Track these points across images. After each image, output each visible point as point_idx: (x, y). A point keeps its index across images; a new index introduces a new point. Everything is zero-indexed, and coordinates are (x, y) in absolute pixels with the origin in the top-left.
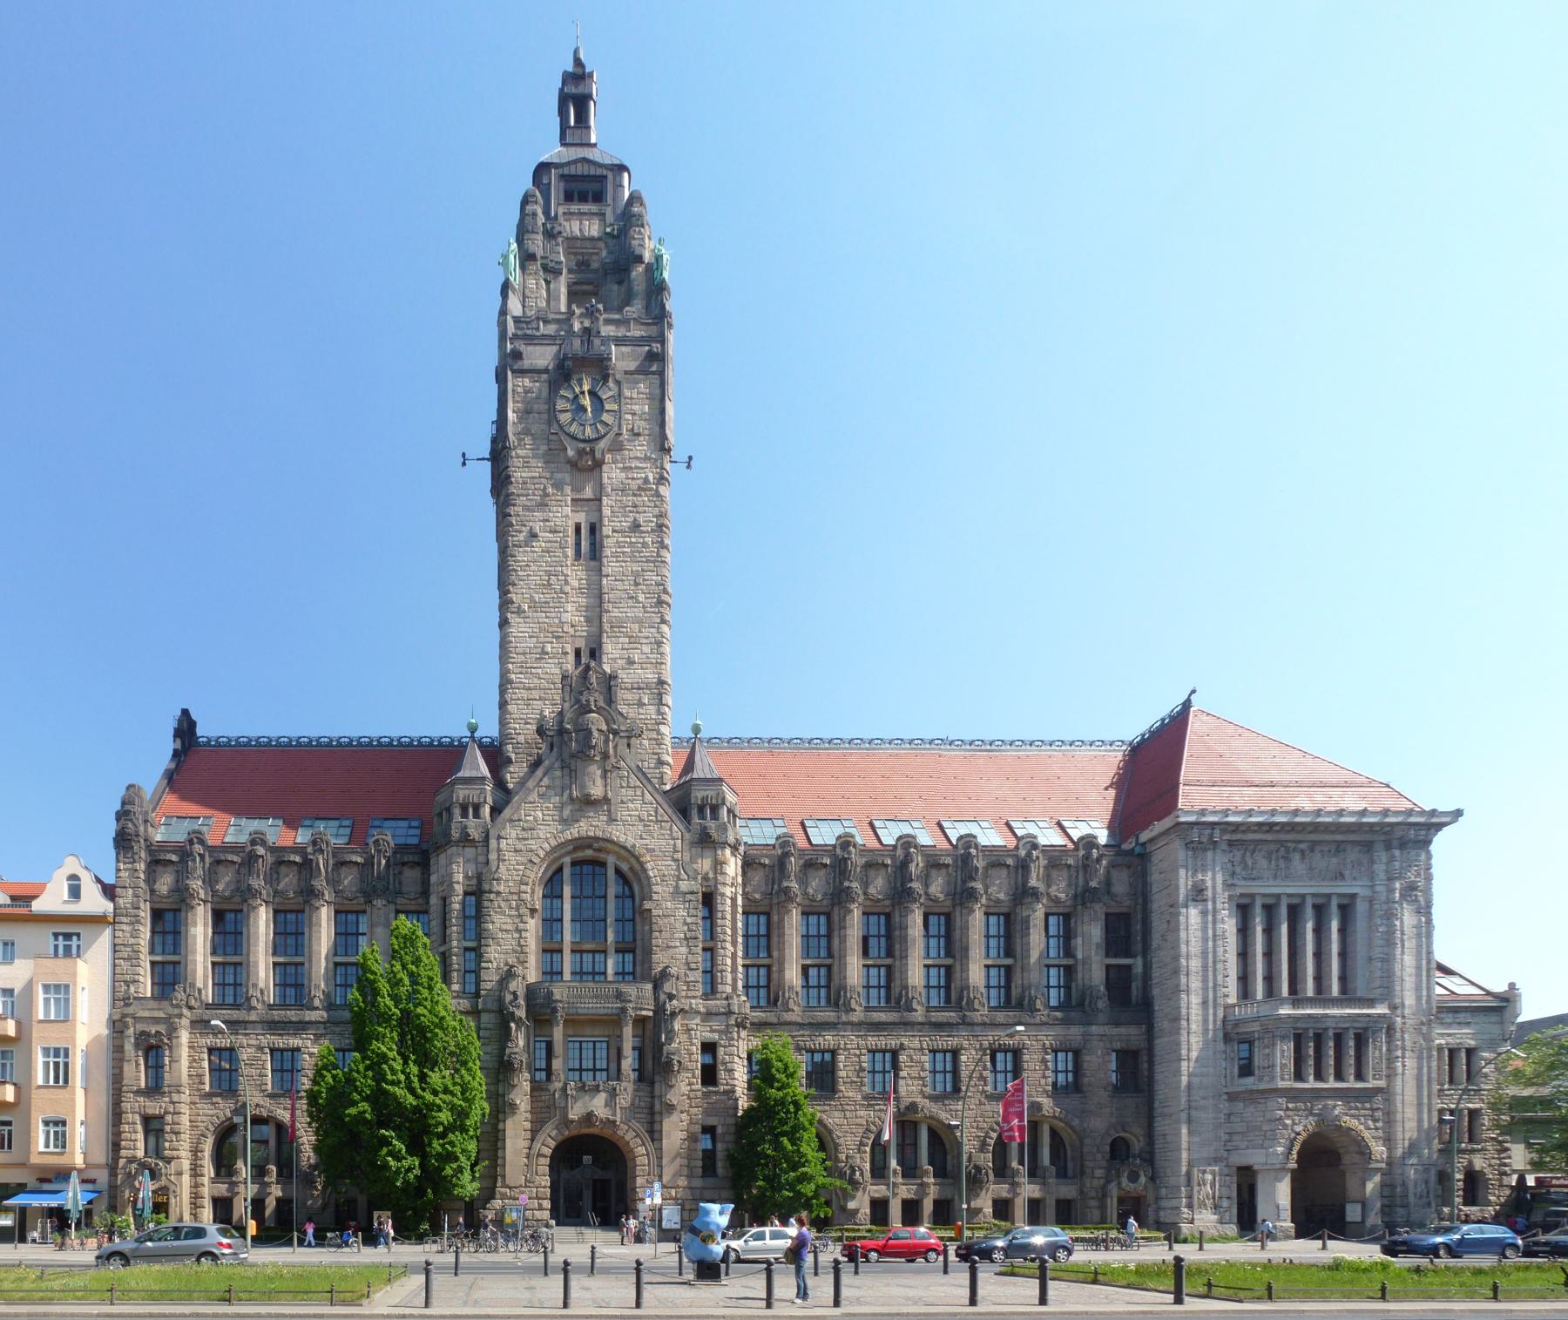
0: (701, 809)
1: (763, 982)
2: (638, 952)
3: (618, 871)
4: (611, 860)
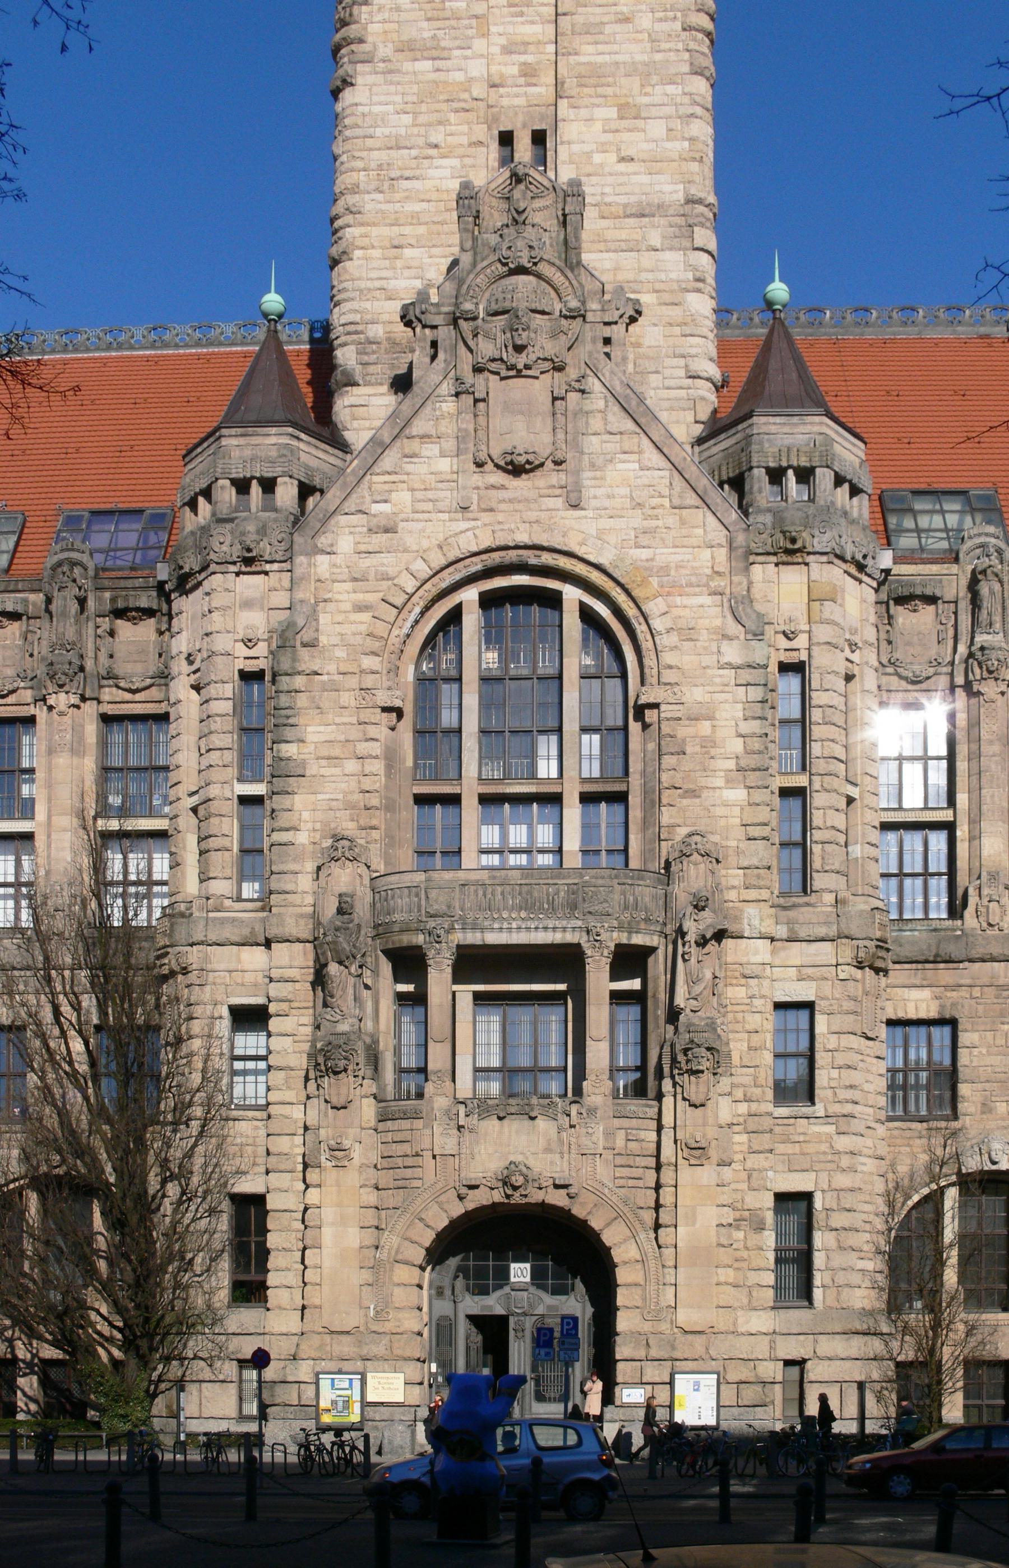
0: (776, 476)
1: (938, 863)
2: (635, 800)
3: (587, 615)
4: (571, 595)
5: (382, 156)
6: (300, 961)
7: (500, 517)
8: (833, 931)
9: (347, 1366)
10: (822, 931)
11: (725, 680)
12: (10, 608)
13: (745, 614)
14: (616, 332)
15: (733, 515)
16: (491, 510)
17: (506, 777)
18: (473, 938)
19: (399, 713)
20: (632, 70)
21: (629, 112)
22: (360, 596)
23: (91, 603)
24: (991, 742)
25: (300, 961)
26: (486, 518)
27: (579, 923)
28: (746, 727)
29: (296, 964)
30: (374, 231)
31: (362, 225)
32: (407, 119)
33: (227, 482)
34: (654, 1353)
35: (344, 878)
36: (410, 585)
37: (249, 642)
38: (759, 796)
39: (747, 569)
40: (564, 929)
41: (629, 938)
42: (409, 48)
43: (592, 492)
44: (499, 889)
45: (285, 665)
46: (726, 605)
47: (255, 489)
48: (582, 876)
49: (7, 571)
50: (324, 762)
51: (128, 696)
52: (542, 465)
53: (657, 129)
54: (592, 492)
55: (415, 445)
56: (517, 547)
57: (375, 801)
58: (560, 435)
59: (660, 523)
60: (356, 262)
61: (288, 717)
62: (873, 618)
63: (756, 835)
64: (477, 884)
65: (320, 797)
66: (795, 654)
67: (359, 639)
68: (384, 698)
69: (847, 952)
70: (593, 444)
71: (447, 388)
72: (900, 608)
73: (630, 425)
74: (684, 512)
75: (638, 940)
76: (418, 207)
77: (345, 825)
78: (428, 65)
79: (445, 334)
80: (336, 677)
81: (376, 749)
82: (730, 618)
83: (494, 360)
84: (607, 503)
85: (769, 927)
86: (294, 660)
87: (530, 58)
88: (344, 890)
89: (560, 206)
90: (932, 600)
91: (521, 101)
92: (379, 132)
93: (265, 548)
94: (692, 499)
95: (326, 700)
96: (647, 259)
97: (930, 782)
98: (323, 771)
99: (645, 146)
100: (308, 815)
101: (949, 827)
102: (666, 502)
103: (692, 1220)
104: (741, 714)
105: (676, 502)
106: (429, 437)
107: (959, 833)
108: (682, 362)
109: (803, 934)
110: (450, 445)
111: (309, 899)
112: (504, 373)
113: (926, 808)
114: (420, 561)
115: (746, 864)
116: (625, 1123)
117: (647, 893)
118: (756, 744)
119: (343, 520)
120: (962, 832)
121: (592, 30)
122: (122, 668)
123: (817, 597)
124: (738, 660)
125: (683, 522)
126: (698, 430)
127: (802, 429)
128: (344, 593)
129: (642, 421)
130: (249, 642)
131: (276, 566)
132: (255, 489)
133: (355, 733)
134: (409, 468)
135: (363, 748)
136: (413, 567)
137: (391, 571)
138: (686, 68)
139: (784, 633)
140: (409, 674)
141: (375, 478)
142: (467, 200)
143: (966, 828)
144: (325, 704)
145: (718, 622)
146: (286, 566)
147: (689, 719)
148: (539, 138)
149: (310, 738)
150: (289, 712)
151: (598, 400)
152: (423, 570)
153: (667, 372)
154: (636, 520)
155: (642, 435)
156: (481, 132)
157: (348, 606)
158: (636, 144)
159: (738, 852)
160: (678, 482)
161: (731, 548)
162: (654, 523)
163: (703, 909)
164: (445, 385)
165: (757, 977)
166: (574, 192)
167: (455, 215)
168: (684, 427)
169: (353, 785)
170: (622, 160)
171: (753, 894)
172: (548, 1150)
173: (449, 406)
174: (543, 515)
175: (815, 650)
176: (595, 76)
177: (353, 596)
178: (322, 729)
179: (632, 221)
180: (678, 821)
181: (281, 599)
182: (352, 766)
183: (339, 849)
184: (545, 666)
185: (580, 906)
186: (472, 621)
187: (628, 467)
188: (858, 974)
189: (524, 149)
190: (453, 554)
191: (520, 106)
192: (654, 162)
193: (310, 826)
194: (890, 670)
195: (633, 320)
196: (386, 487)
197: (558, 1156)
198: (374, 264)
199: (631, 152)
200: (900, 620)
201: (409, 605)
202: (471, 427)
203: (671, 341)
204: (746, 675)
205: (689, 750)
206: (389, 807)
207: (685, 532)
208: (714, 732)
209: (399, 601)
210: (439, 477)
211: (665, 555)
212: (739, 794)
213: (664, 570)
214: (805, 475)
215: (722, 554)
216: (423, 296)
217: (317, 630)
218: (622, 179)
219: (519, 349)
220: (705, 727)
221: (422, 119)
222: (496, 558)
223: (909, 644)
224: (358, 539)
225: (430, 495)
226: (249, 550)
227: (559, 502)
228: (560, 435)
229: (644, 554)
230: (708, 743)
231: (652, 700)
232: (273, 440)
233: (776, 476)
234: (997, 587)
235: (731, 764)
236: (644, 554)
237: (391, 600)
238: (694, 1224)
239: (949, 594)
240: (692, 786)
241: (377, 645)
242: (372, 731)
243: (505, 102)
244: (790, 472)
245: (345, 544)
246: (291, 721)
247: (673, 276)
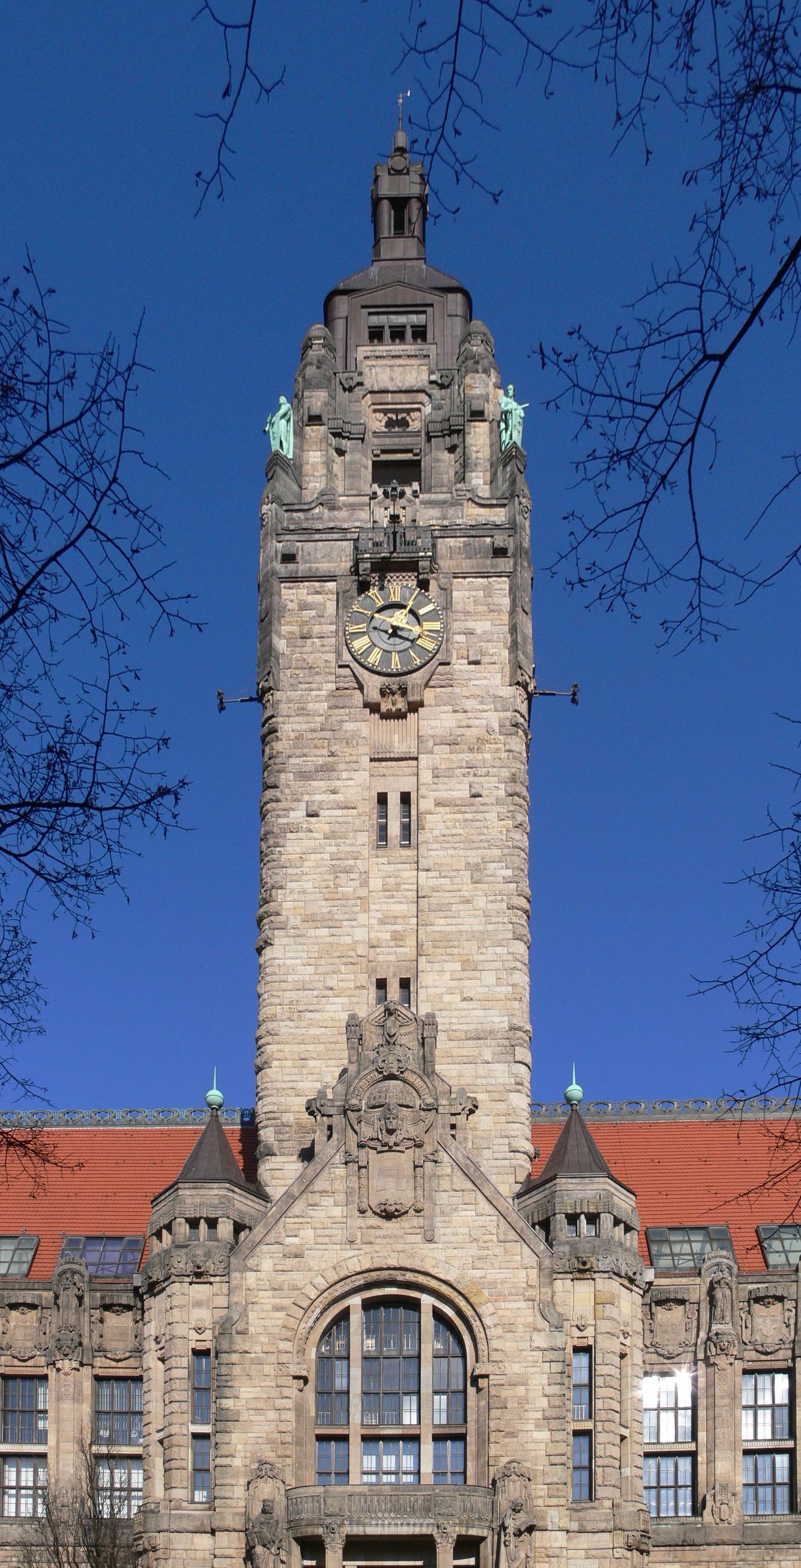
0: (572, 1219)
1: (685, 1478)
2: (471, 1439)
3: (438, 1315)
4: (427, 1301)
5: (293, 995)
6: (236, 1544)
7: (377, 1248)
8: (611, 1525)
10: (603, 1526)
11: (535, 1359)
12: (29, 1301)
13: (551, 1315)
14: (460, 1120)
15: (542, 1247)
16: (371, 1243)
17: (381, 1423)
18: (358, 1530)
19: (306, 1380)
20: (472, 936)
21: (469, 966)
22: (278, 1301)
23: (86, 1299)
24: (723, 1397)
25: (236, 1544)
26: (367, 1248)
27: (432, 1521)
28: (550, 1390)
29: (233, 1546)
30: (287, 1048)
31: (278, 1043)
32: (310, 969)
33: (183, 1220)
35: (266, 1489)
36: (313, 1294)
37: (199, 1330)
38: (560, 1436)
39: (551, 1284)
40: (421, 1525)
41: (467, 1531)
42: (312, 920)
43: (442, 1231)
44: (376, 1498)
45: (225, 1346)
46: (536, 1308)
47: (203, 1225)
48: (434, 1490)
49: (27, 1275)
50: (252, 1412)
51: (113, 1364)
52: (407, 1212)
53: (489, 978)
54: (442, 1231)
55: (316, 1198)
56: (388, 1269)
57: (288, 1438)
58: (420, 1192)
59: (490, 1252)
60: (274, 1070)
61: (227, 1381)
62: (640, 1315)
63: (557, 1462)
64: (360, 1494)
65: (250, 1435)
66: (585, 1340)
67: (277, 1330)
68: (294, 1370)
69: (620, 1539)
70: (443, 1198)
71: (339, 1158)
72: (659, 1308)
73: (470, 1185)
74: (507, 1244)
75: (473, 1532)
76: (319, 1031)
77: (267, 1454)
78: (325, 932)
79: (338, 1121)
80: (261, 1355)
81: (289, 1404)
82: (539, 1317)
83: (372, 1139)
84: (452, 1239)
85: (565, 1523)
86: (231, 1342)
87: (398, 928)
88: (266, 1497)
89: (420, 1032)
90: (682, 1302)
91: (392, 958)
92: (290, 978)
93: (210, 1266)
94: (513, 1236)
95: (254, 1370)
96: (482, 1069)
97: (679, 1424)
98: (251, 1418)
99: (481, 990)
100: (241, 1447)
101: (693, 1455)
102: (494, 1238)
104: (546, 1382)
105: (502, 1238)
106: (327, 1192)
107: (699, 1459)
108: (506, 1141)
109: (589, 1528)
110: (341, 1198)
111: (242, 1503)
112: (380, 1148)
113: (676, 1442)
114: (320, 1277)
115: (549, 1481)
117: (479, 1501)
118: (557, 1401)
119: (265, 1248)
120: (701, 1458)
121: (442, 909)
122: (109, 1345)
123: (599, 1302)
124: (544, 1345)
125: (506, 1252)
126: (518, 1188)
127: (591, 1187)
128: (266, 1299)
129: (478, 1182)
130: (199, 1330)
131: (218, 1279)
132: (203, 1225)
133: (274, 1393)
134: (312, 1213)
135: (280, 1403)
136: (315, 1282)
137: (300, 1284)
138: (510, 935)
139: (577, 1326)
140: (312, 1354)
141: (288, 1220)
142: (353, 1026)
143: (705, 1455)
144: (253, 1373)
145: (531, 1320)
146: (225, 1279)
147: (510, 1385)
148: (405, 984)
149: (242, 1395)
150: (228, 1378)
151: (446, 1167)
152: (322, 1284)
153: (496, 1148)
155: (478, 1192)
156: (363, 979)
157: (269, 1307)
158: (474, 988)
159: (544, 1473)
160: (503, 1224)
161: (540, 1269)
162: (486, 1252)
163: (519, 1511)
164: (338, 1156)
165: (557, 1556)
166: (430, 1022)
167: (345, 1037)
168: (507, 1186)
169: (273, 1428)
170: (464, 999)
171: (554, 1501)
173: (341, 1171)
174: (407, 1247)
175: (599, 1338)
176: (445, 941)
177: (272, 1300)
178: (251, 1389)
179: (471, 1042)
180: (502, 1453)
181: (222, 1301)
182: (272, 1415)
183: (262, 1470)
184: (408, 1349)
185: (433, 1509)
186: (356, 1318)
187: (467, 1215)
188: (628, 1554)
189: (394, 992)
191: (391, 961)
192: (487, 1001)
193: (242, 1454)
194: (652, 1350)
195: (472, 1112)
196: (296, 1226)
198: (287, 1071)
199: (471, 994)
200: (659, 1316)
201: (312, 1307)
202: (356, 1186)
203: (499, 1127)
204: (550, 1355)
205: (509, 1405)
206: (299, 1442)
207: (507, 1258)
208: (527, 1393)
209: (305, 1304)
210: (334, 1220)
212: (545, 1435)
213: (493, 1284)
214: (593, 1218)
215: (534, 1273)
216: (322, 1094)
218: (464, 1013)
219: (391, 1132)
220: (521, 1390)
221: (321, 969)
222: (374, 1275)
223: (665, 1332)
224: (276, 1261)
225: (327, 1232)
226: (199, 1267)
227: (419, 1238)
228: (420, 1192)
229: (478, 1273)
230: (523, 1401)
231: (483, 1372)
232: (215, 1192)
233: (572, 1219)
234: (728, 1292)
235: (539, 1415)
236: (478, 1273)
237: (299, 1303)
239: (694, 1298)
240: (511, 1430)
241: (290, 1334)
242: (286, 1392)
243: (381, 958)
244: (583, 1217)
245: (267, 1265)
246: (229, 1384)
247: (501, 1081)
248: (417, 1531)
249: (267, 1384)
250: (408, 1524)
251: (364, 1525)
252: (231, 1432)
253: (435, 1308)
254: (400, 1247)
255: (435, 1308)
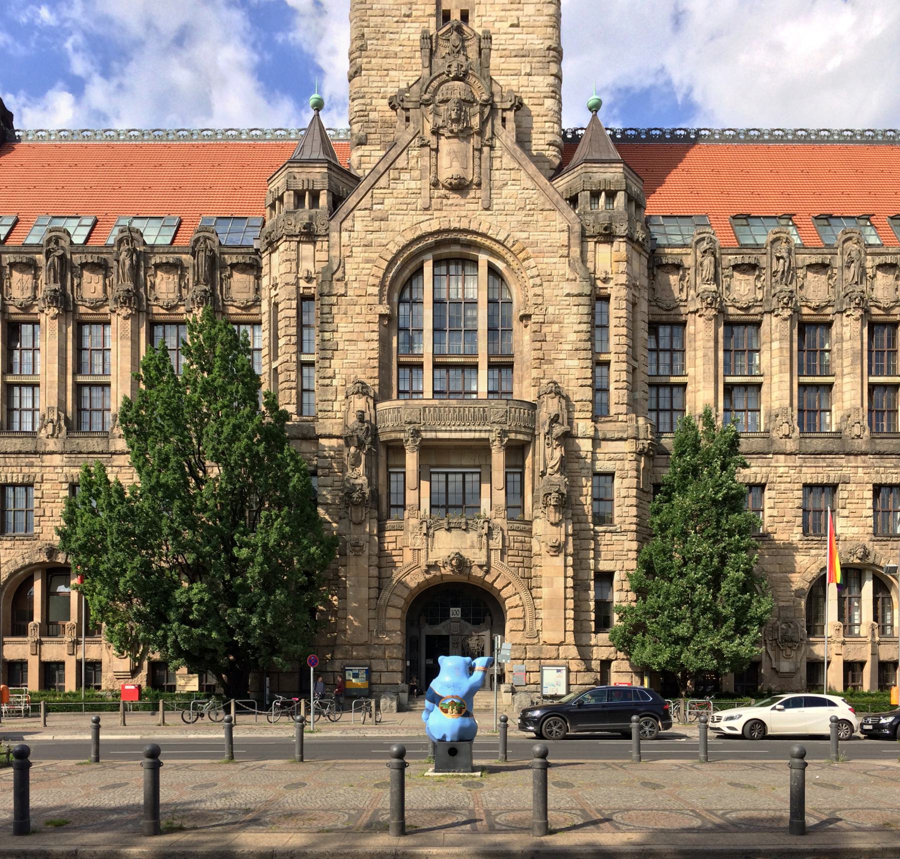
7: (444, 213)
9: (361, 662)
26: (437, 214)
34: (529, 655)
48: (490, 403)
67: (366, 278)
75: (520, 437)
86: (331, 286)
103: (551, 584)
109: (608, 436)
110: (416, 173)
116: (514, 533)
133: (365, 327)
141: (375, 191)
154: (520, 216)
157: (360, 260)
162: (530, 218)
172: (472, 547)
182: (362, 345)
190: (418, 233)
196: (382, 196)
197: (477, 551)
205: (547, 339)
207: (547, 223)
209: (389, 258)
211: (535, 236)
212: (575, 363)
213: (535, 244)
217: (344, 273)
220: (555, 327)
233: (595, 195)
238: (552, 586)
244: (603, 194)
248: (477, 435)
249: (359, 320)
250: (470, 431)
251: (436, 431)
252: (330, 359)
253: (489, 262)
254: (464, 213)
255: (489, 262)
